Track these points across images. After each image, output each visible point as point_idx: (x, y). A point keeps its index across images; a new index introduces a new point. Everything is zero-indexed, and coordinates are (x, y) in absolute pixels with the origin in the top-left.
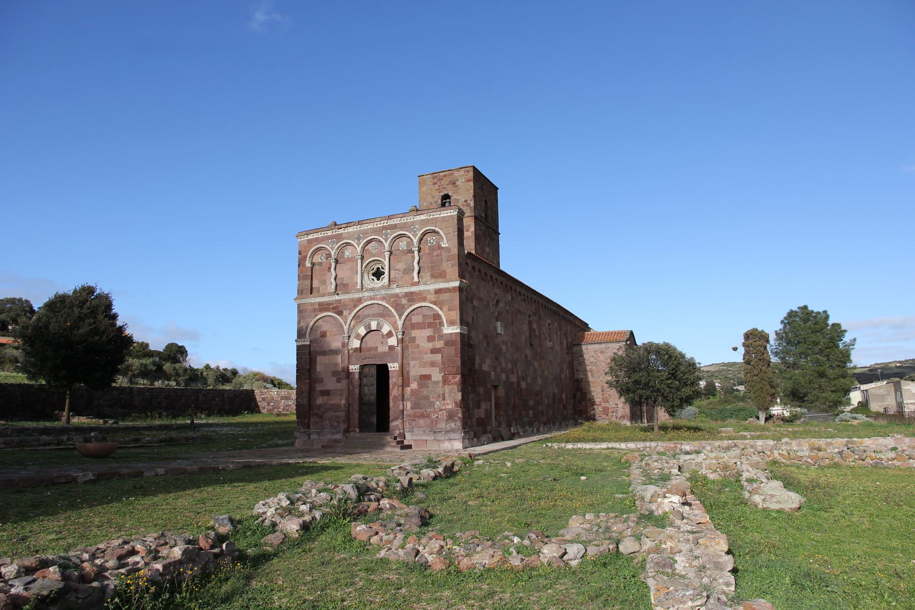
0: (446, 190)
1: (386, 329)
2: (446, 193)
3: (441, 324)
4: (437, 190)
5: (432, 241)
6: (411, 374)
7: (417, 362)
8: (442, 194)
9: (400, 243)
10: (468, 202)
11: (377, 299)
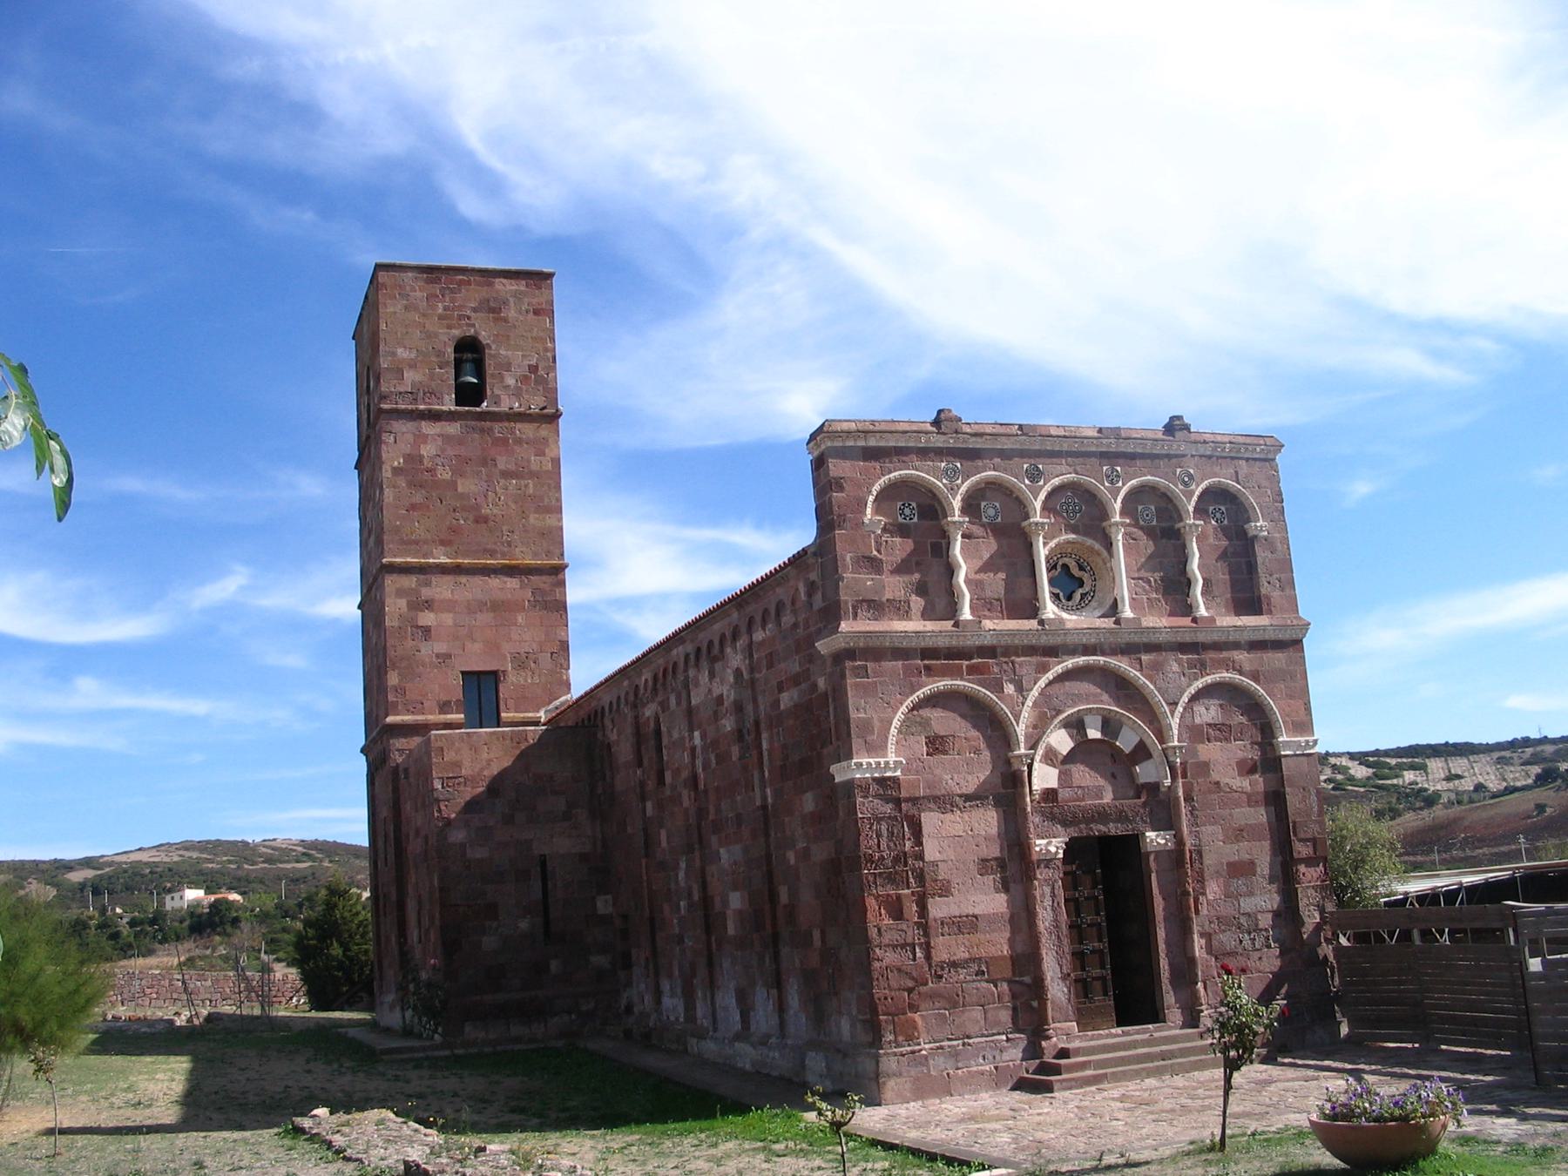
0: (468, 325)
1: (1126, 742)
4: (441, 318)
5: (1218, 515)
6: (1208, 860)
7: (1217, 829)
8: (457, 333)
9: (1140, 508)
10: (541, 372)
11: (1103, 654)
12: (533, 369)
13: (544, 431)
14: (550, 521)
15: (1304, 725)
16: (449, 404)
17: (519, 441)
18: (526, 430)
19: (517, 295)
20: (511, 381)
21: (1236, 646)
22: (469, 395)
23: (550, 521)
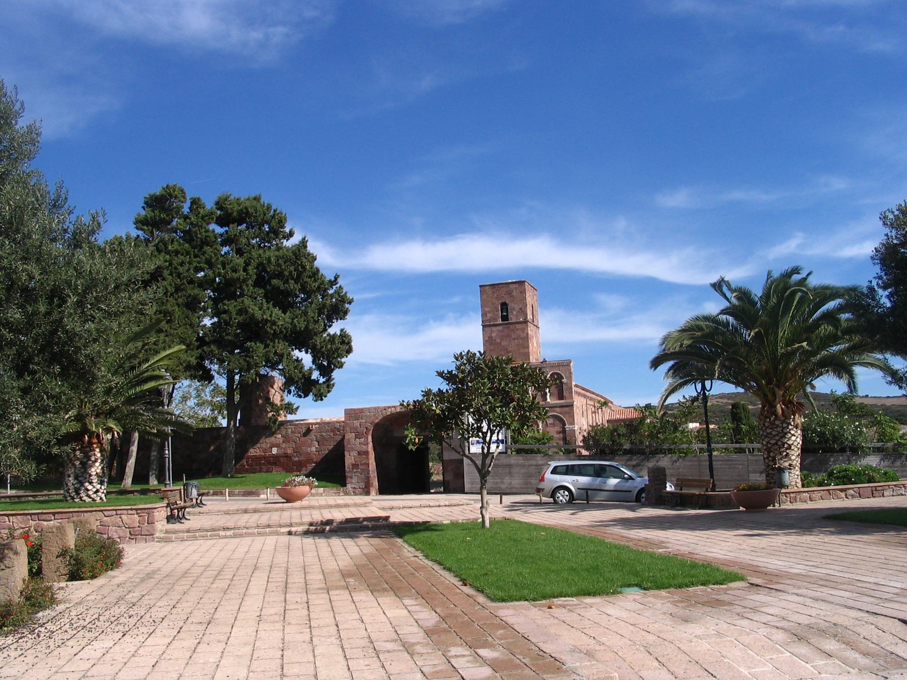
2: (504, 301)
3: (564, 424)
4: (496, 298)
8: (500, 301)
10: (523, 309)
12: (521, 309)
13: (524, 326)
14: (526, 350)
15: (573, 423)
16: (500, 321)
17: (517, 330)
18: (518, 326)
19: (516, 288)
20: (515, 313)
21: (556, 407)
22: (505, 318)
23: (526, 350)
